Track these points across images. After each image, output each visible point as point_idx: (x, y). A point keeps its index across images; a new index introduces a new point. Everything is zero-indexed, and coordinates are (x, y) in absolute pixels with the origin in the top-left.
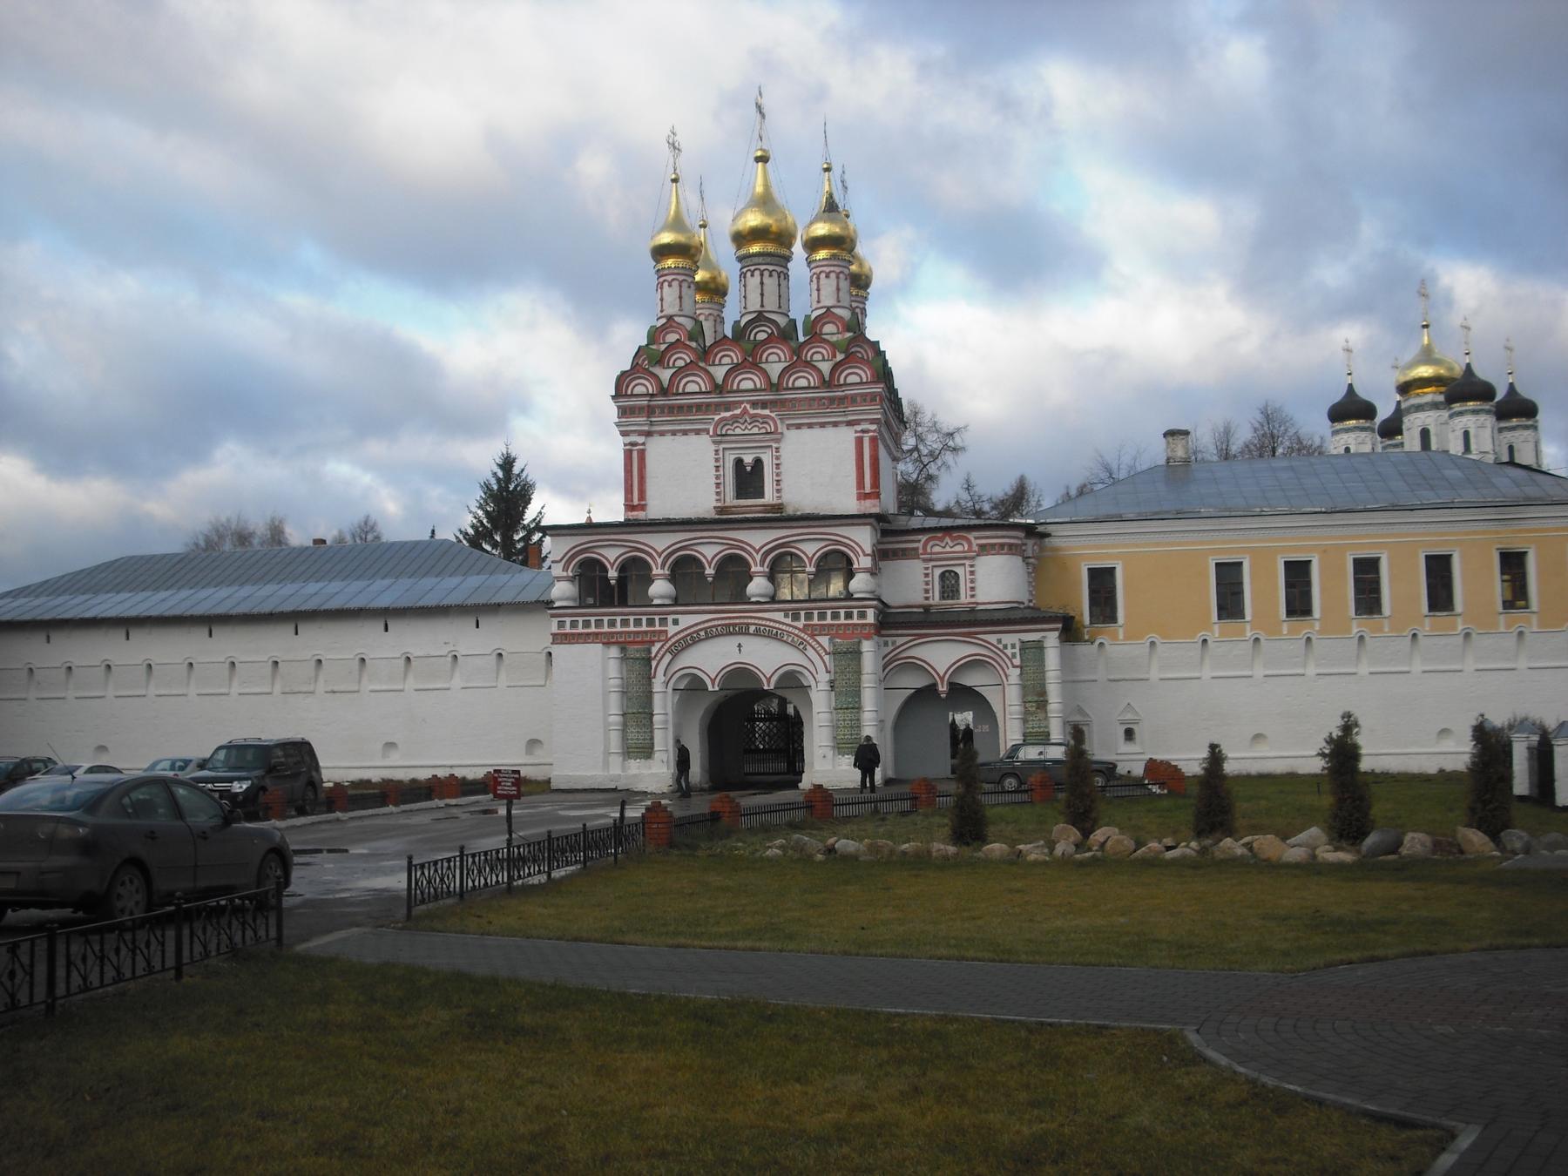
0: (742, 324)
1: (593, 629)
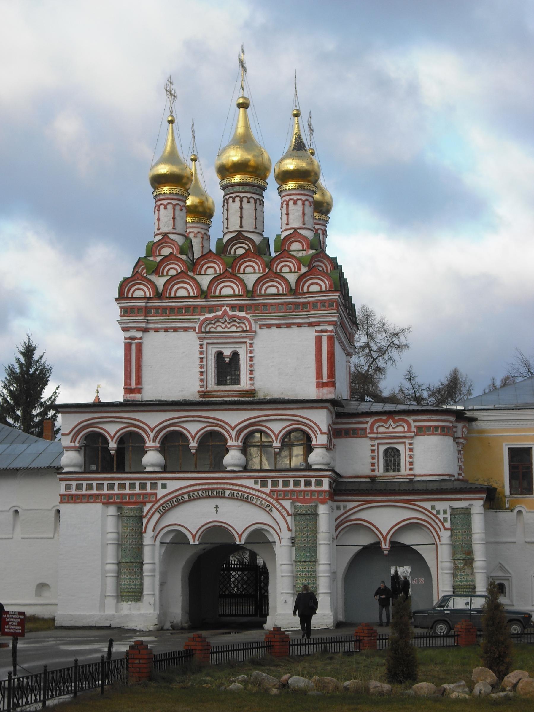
0: (225, 241)
1: (95, 491)
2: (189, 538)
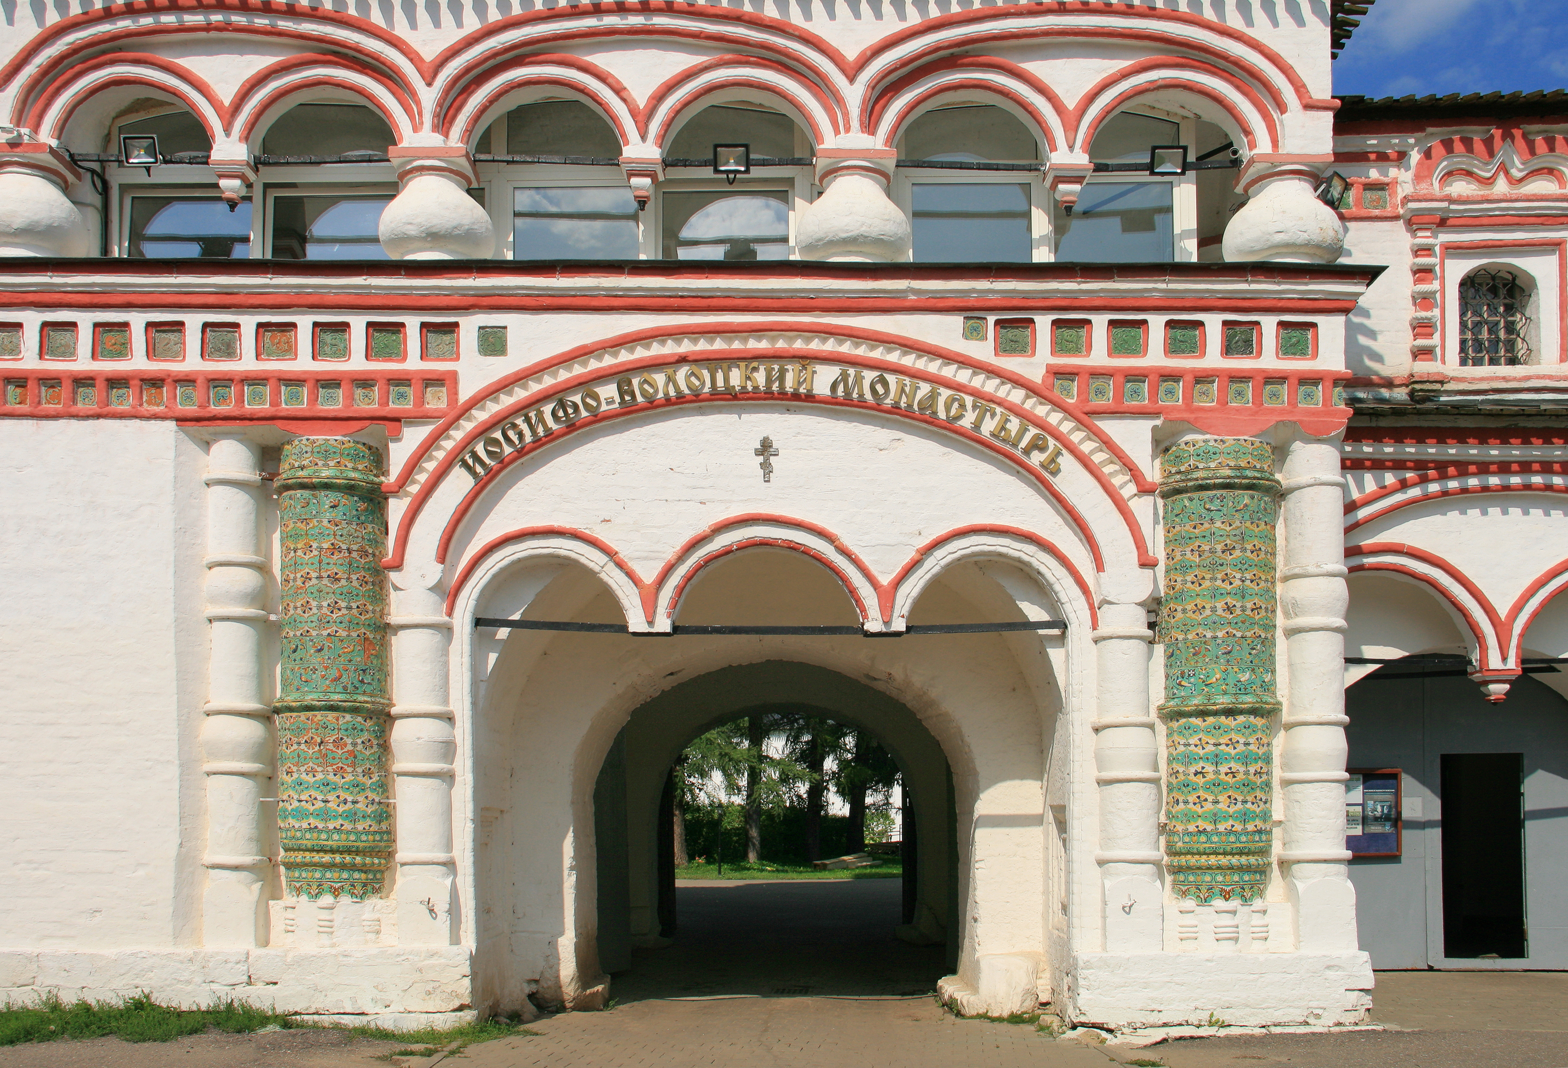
2: (625, 602)
